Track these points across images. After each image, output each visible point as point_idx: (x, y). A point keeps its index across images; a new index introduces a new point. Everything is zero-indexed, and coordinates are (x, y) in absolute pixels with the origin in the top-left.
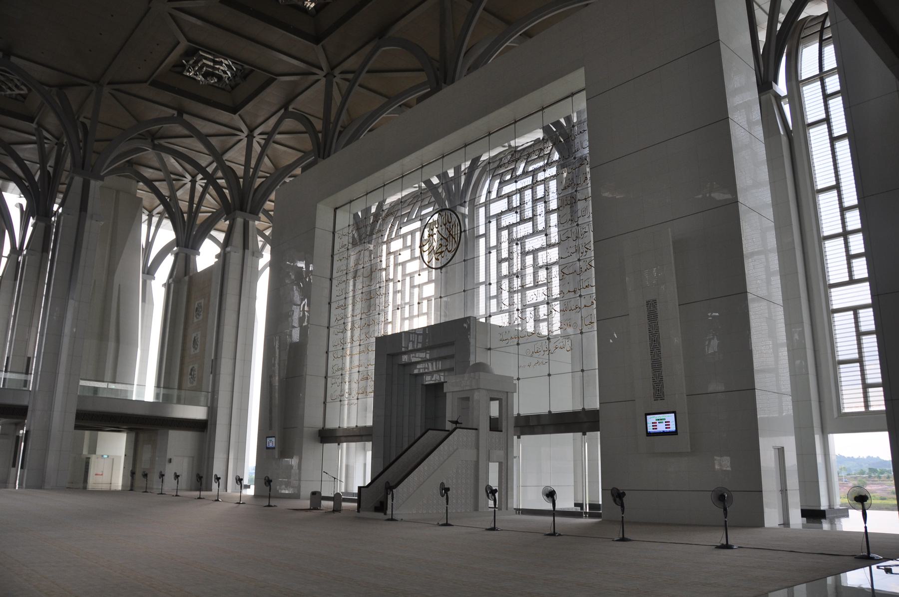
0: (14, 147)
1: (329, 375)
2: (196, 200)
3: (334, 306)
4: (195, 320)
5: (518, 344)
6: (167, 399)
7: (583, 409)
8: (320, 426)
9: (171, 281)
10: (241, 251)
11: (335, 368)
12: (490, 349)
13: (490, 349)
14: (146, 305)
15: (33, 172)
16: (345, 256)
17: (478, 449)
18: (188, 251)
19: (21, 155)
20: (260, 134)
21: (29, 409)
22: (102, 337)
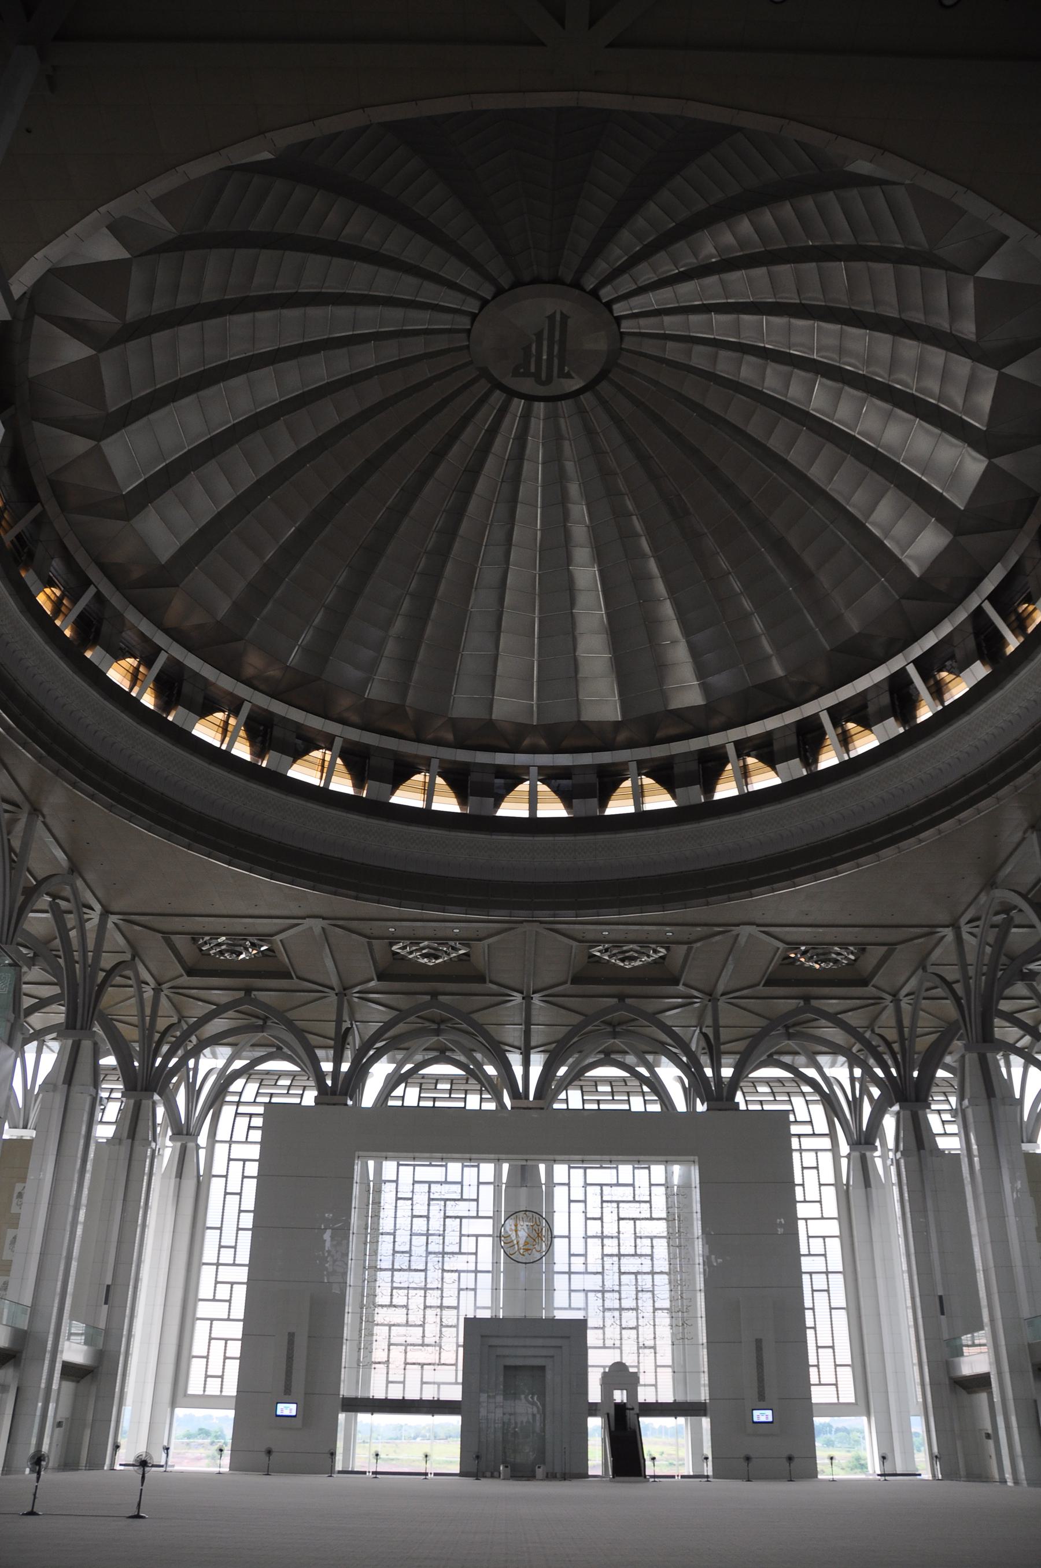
0: (659, 1016)
2: (906, 1022)
9: (899, 1155)
14: (874, 1190)
15: (686, 1039)
19: (669, 1023)
20: (969, 922)
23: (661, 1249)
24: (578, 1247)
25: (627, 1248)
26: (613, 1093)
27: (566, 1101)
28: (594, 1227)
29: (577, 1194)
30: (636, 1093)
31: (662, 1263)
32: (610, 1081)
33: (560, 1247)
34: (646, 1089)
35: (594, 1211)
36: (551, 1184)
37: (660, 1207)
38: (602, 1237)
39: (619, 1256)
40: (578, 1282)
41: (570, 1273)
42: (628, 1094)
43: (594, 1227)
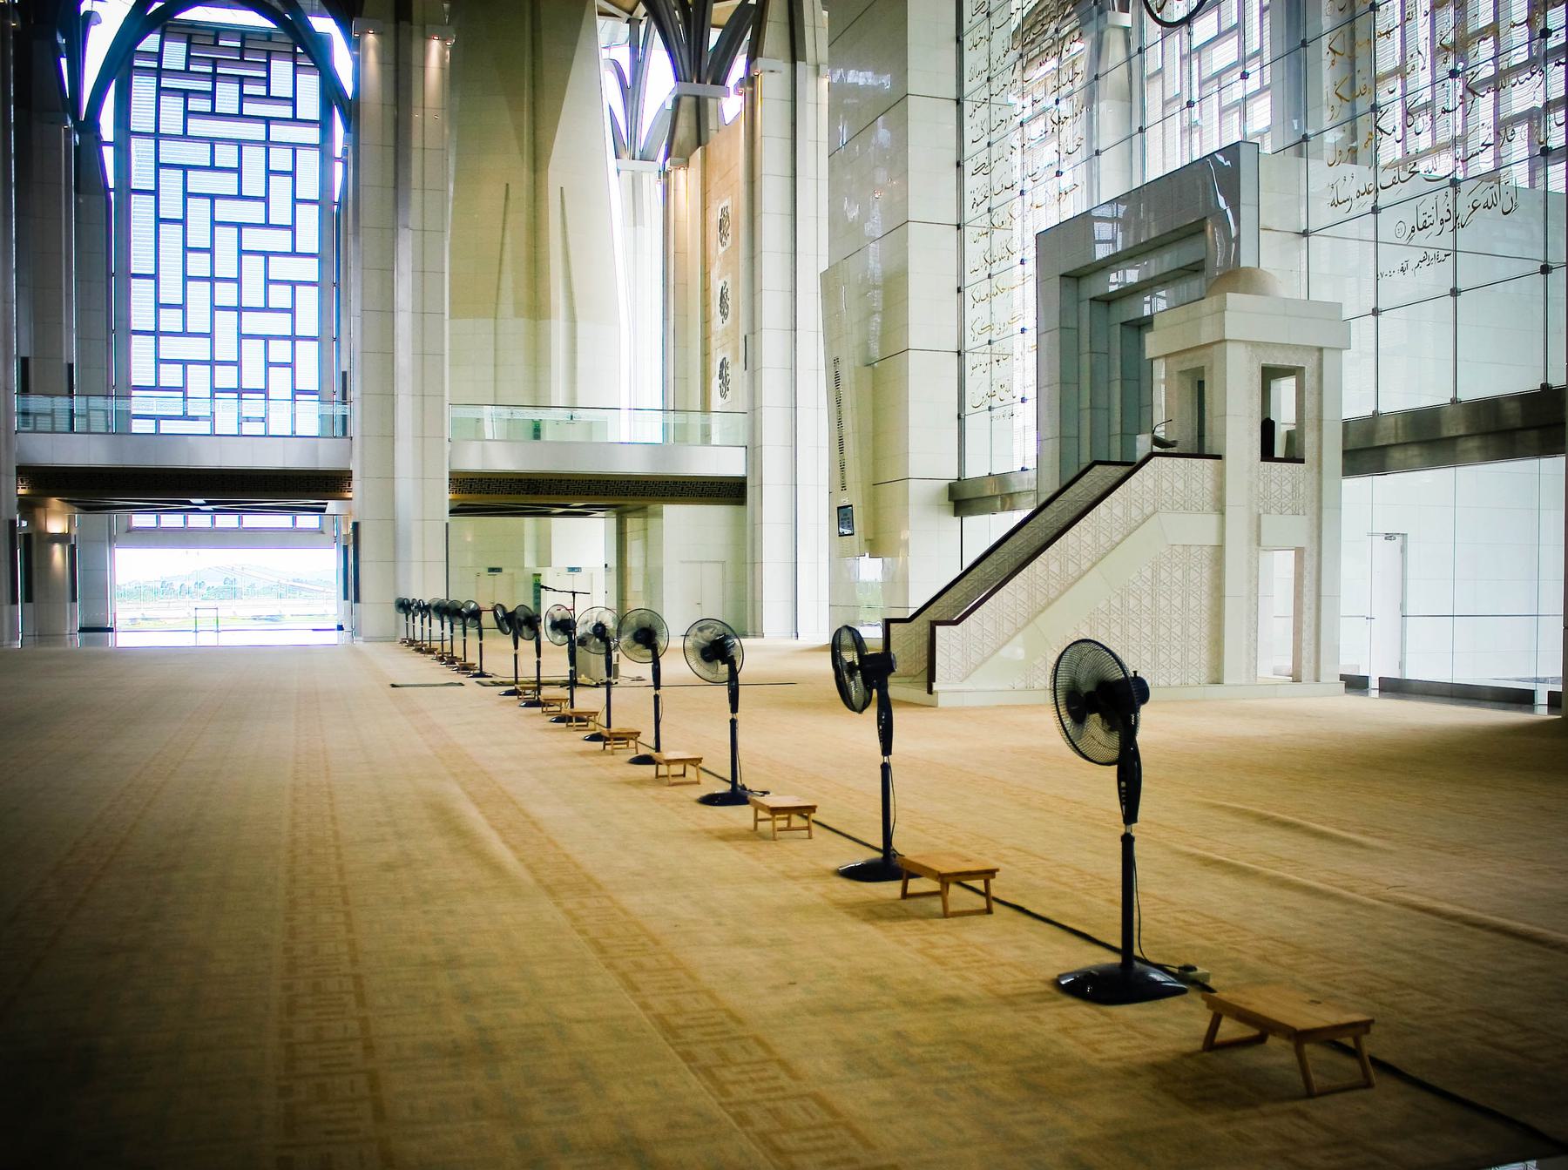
1: (969, 345)
3: (969, 167)
4: (721, 250)
5: (1375, 210)
6: (681, 433)
7: (1545, 387)
8: (953, 474)
10: (786, 67)
11: (978, 327)
12: (1306, 234)
13: (1306, 234)
16: (985, 33)
17: (1220, 508)
18: (706, 89)
21: (355, 476)
22: (536, 309)
23: (308, 300)
24: (171, 294)
25: (253, 297)
26: (242, 51)
27: (159, 56)
28: (198, 264)
29: (171, 208)
30: (282, 55)
31: (308, 323)
32: (244, 34)
33: (141, 292)
34: (299, 50)
35: (198, 237)
36: (126, 189)
37: (309, 239)
38: (212, 279)
39: (240, 309)
40: (171, 348)
41: (157, 333)
42: (269, 55)
43: (198, 264)
